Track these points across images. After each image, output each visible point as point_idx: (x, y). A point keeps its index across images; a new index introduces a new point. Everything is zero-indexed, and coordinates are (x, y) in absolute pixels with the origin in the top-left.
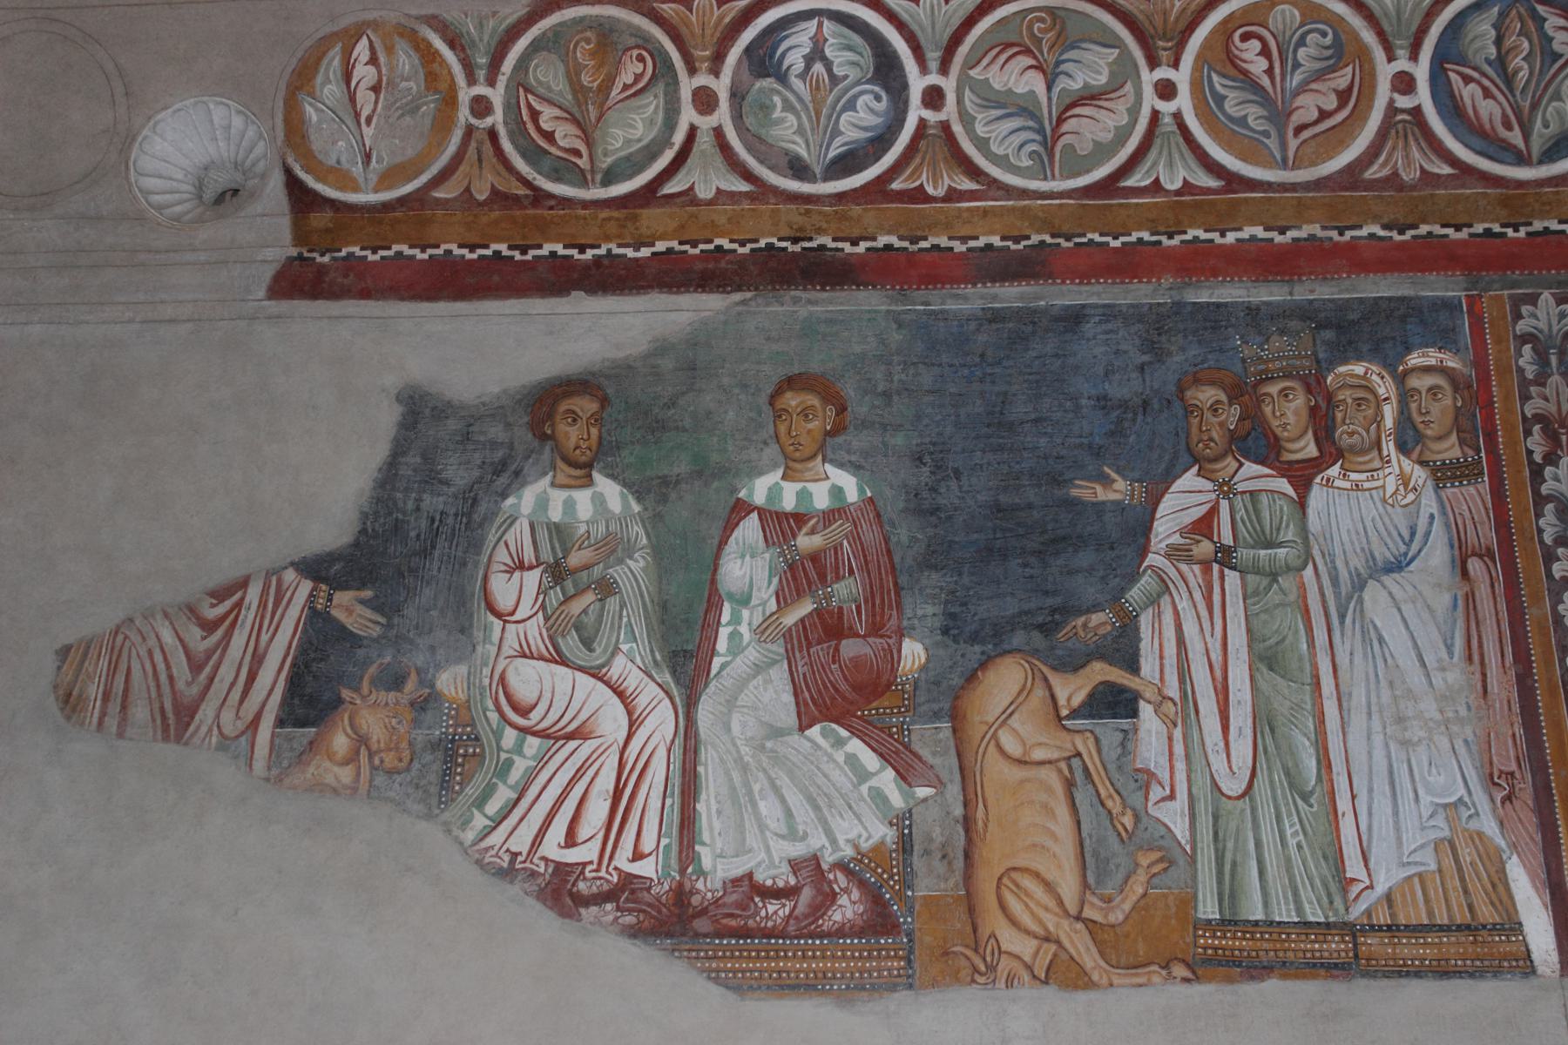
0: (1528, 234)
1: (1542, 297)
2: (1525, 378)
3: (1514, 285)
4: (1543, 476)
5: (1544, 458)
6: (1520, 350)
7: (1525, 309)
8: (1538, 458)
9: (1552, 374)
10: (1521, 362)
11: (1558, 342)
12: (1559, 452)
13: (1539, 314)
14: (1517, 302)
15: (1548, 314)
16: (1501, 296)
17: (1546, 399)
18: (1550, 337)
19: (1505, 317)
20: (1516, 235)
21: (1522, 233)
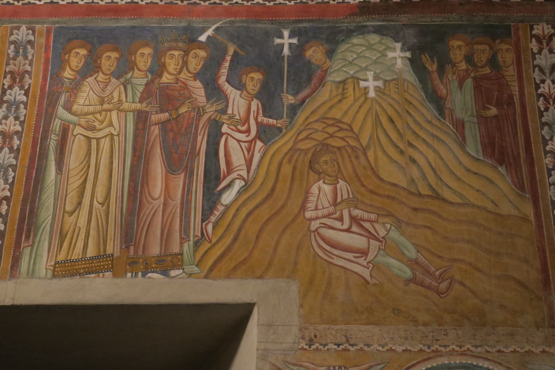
0: (23, 4)
1: (22, 27)
2: (9, 57)
3: (14, 23)
4: (6, 93)
5: (8, 87)
6: (10, 47)
7: (15, 32)
8: (6, 87)
9: (18, 56)
10: (9, 51)
11: (24, 44)
12: (15, 85)
13: (19, 34)
14: (13, 29)
15: (23, 34)
16: (7, 27)
17: (15, 65)
18: (22, 42)
19: (7, 35)
20: (18, 4)
21: (20, 3)
